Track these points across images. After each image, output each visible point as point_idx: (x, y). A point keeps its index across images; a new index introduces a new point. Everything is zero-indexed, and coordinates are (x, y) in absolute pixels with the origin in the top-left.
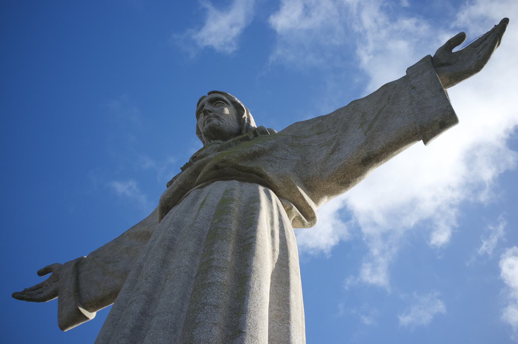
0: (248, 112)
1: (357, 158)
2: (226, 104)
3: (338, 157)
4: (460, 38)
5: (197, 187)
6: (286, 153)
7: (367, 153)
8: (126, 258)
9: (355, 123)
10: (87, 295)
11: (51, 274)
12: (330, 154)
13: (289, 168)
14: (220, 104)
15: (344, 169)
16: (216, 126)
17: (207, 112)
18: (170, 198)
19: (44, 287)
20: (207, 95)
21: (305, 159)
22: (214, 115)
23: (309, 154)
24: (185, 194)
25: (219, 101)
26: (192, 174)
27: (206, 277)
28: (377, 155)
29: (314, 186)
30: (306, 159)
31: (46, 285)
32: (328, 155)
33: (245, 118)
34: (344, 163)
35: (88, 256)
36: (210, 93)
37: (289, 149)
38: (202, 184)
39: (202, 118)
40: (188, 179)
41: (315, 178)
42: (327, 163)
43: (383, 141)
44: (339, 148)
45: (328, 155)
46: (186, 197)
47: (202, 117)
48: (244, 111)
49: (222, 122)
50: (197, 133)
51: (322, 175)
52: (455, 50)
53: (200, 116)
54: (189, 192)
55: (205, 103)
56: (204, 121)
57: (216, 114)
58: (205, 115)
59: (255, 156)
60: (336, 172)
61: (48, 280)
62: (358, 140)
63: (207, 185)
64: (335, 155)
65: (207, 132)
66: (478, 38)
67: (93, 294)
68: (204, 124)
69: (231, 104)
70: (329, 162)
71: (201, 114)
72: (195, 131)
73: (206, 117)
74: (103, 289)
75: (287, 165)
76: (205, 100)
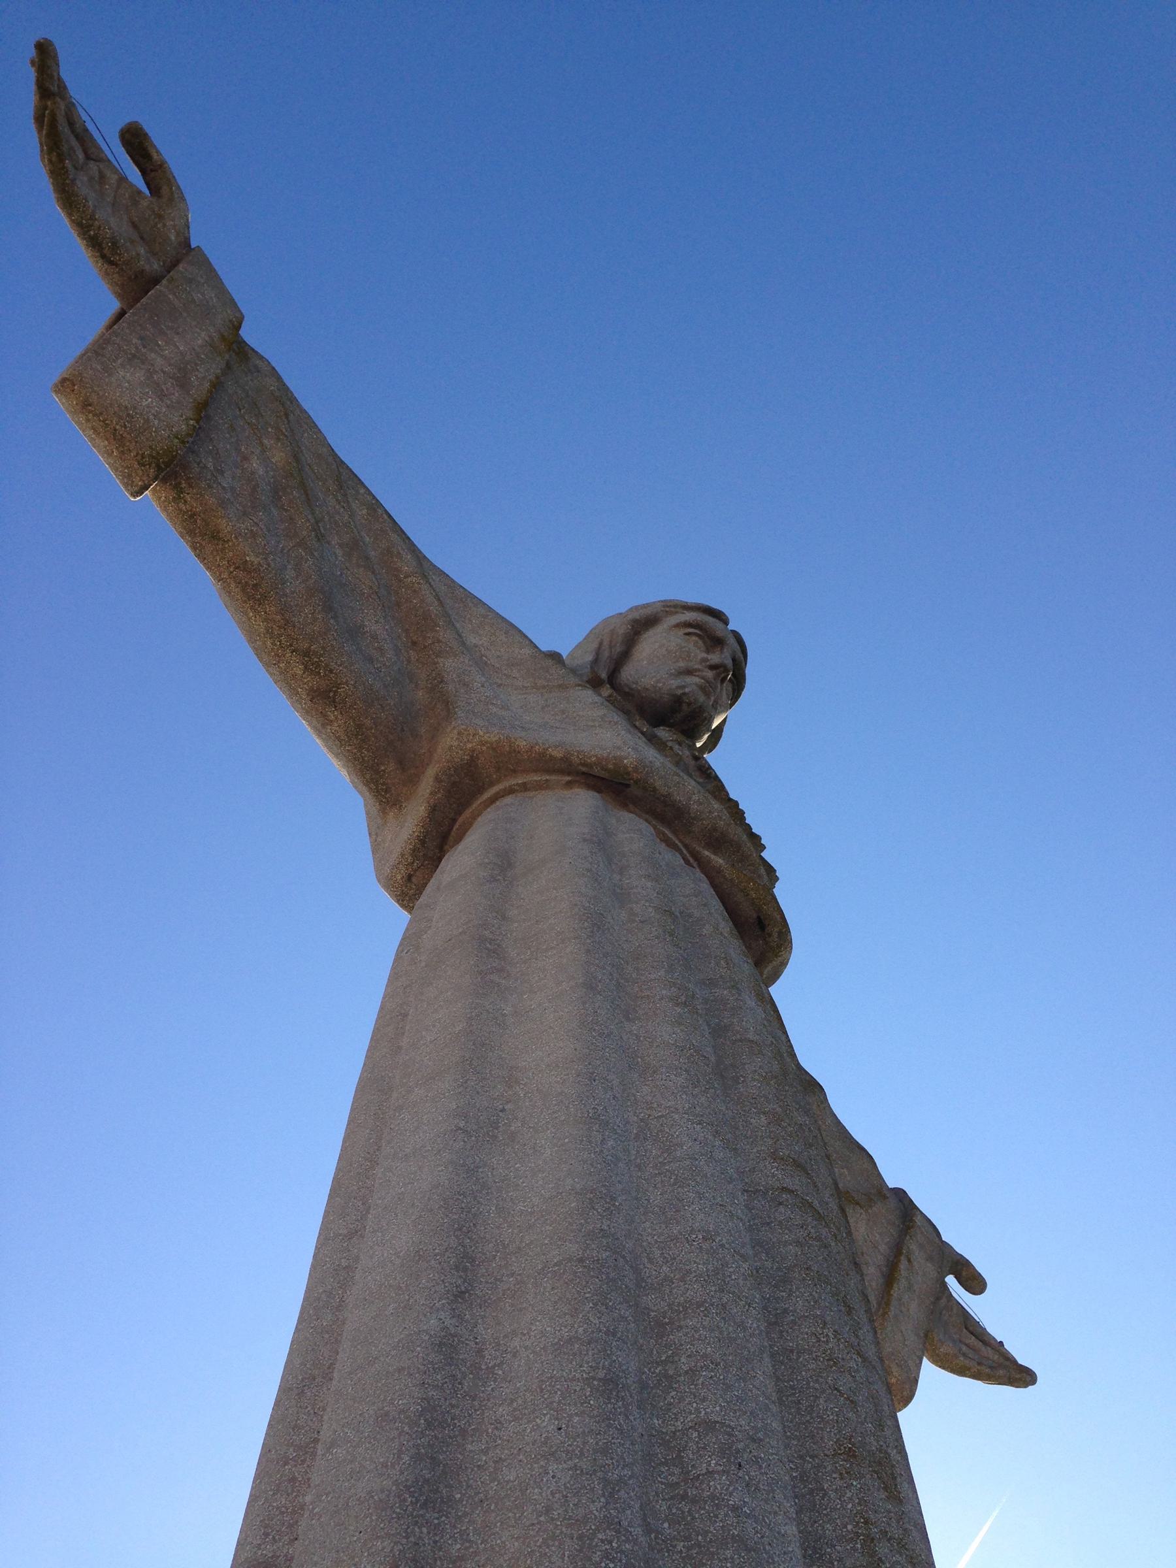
4: (975, 1283)
16: (707, 726)
18: (655, 790)
19: (92, 164)
20: (731, 627)
36: (736, 635)
52: (951, 1280)
53: (694, 638)
56: (699, 670)
61: (123, 179)
65: (689, 704)
66: (978, 1320)
68: (689, 672)
71: (700, 642)
73: (710, 674)
74: (255, 529)
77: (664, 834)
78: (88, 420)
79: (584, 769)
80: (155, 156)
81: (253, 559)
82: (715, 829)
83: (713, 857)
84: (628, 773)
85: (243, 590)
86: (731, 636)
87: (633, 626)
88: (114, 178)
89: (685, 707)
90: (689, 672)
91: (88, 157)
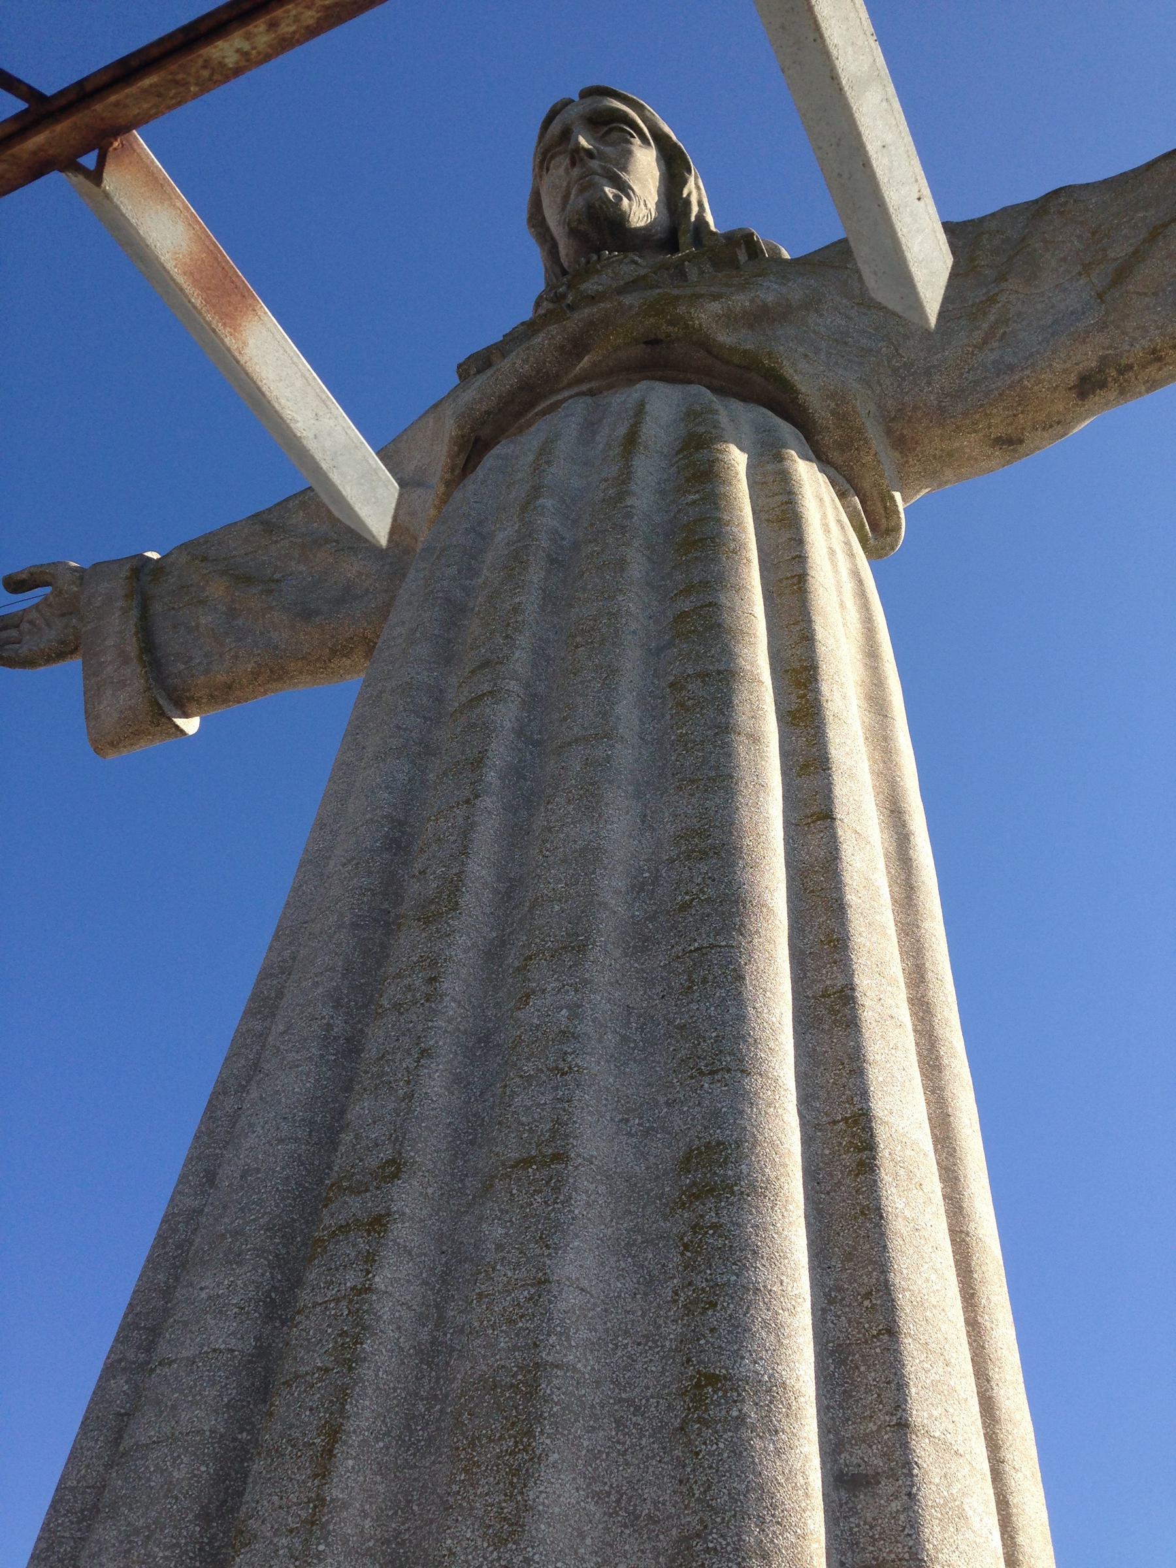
0: (696, 178)
1: (1065, 371)
2: (637, 141)
3: (1001, 357)
5: (576, 390)
6: (843, 323)
7: (1100, 357)
8: (301, 573)
9: (1064, 259)
10: (182, 667)
11: (47, 590)
12: (975, 347)
13: (856, 371)
14: (619, 134)
15: (1017, 399)
17: (582, 154)
18: (488, 413)
19: (25, 626)
20: (576, 98)
21: (897, 350)
22: (603, 168)
23: (908, 338)
24: (532, 405)
25: (614, 125)
26: (563, 346)
27: (706, 652)
28: (1129, 367)
29: (913, 438)
30: (901, 351)
31: (31, 622)
32: (970, 349)
33: (689, 195)
34: (1021, 379)
35: (170, 553)
36: (588, 93)
37: (853, 313)
38: (594, 384)
39: (561, 171)
40: (550, 363)
41: (919, 414)
42: (962, 374)
43: (1158, 328)
44: (1005, 333)
45: (970, 349)
46: (544, 413)
47: (560, 168)
48: (689, 171)
49: (629, 198)
50: (530, 220)
51: (945, 407)
53: (552, 166)
54: (559, 397)
55: (572, 123)
56: (569, 183)
57: (609, 166)
58: (573, 163)
59: (760, 317)
60: (991, 405)
61: (36, 607)
62: (1072, 313)
63: (610, 387)
64: (992, 350)
67: (200, 664)
68: (566, 197)
69: (651, 141)
70: (968, 372)
72: (525, 216)
73: (576, 172)
74: (232, 654)
75: (850, 361)
76: (572, 113)
77: (537, 414)
78: (125, 747)
79: (457, 472)
80: (24, 576)
81: (250, 666)
82: (562, 348)
83: (581, 365)
84: (463, 436)
85: (275, 680)
86: (588, 100)
87: (533, 227)
88: (34, 615)
89: (582, 227)
90: (566, 197)
91: (17, 626)
